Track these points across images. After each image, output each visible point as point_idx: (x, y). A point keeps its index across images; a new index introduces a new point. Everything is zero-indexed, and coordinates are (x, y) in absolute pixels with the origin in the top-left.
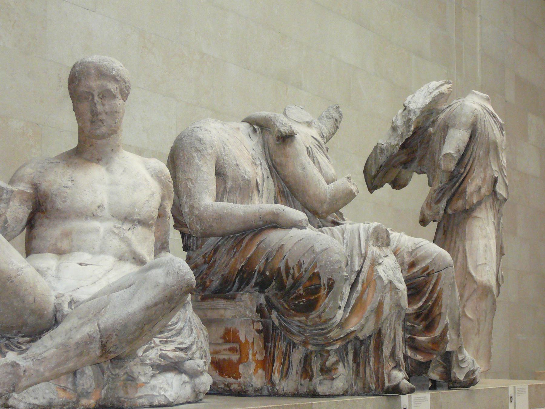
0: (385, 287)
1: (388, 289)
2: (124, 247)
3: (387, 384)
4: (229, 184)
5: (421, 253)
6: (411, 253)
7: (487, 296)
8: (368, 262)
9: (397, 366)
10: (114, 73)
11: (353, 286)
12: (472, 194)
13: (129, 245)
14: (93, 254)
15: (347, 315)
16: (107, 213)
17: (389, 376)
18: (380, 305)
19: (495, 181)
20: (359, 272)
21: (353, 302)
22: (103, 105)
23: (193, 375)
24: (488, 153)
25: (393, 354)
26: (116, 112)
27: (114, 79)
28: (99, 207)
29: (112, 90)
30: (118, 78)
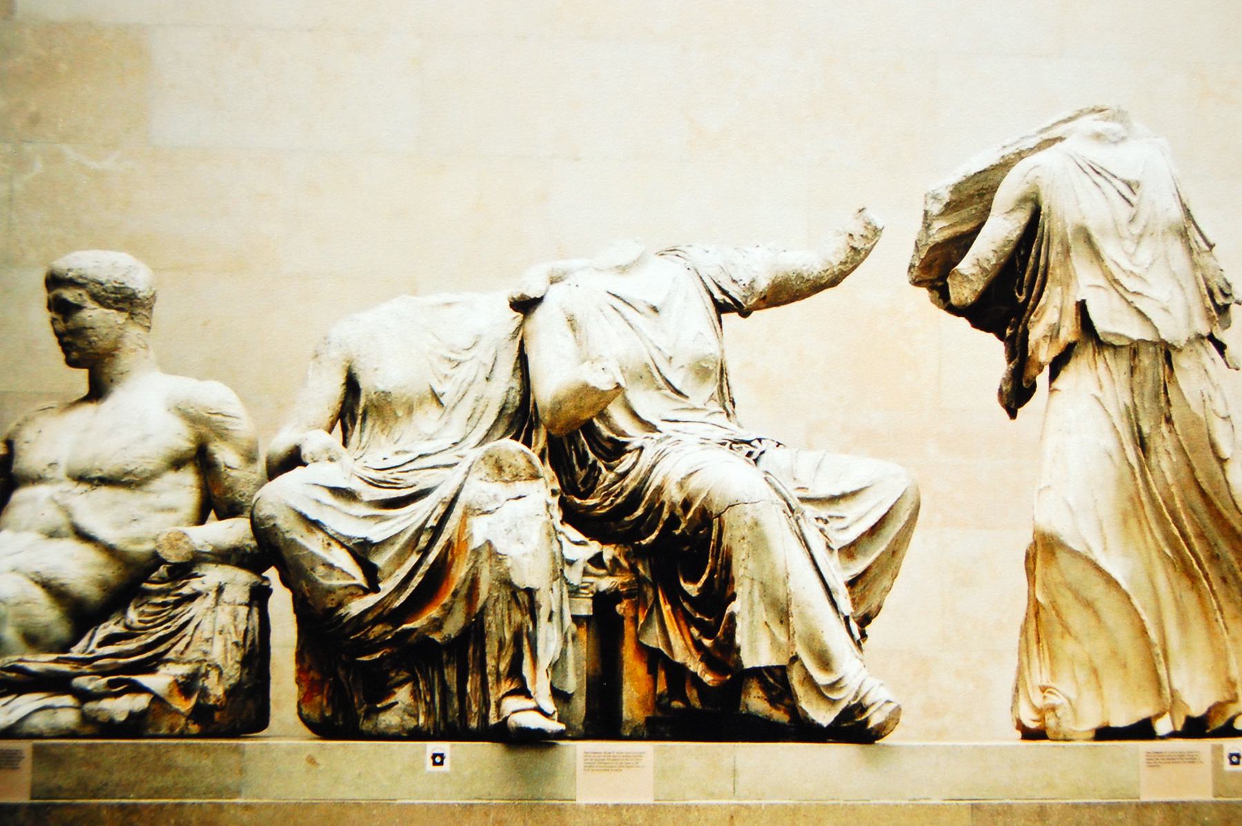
0: (477, 552)
1: (485, 555)
2: (60, 520)
3: (493, 720)
4: (362, 402)
5: (693, 484)
6: (681, 485)
7: (1053, 554)
8: (458, 511)
9: (523, 691)
10: (70, 275)
11: (426, 552)
12: (1037, 344)
13: (69, 515)
14: (17, 530)
15: (397, 604)
16: (61, 472)
17: (498, 705)
18: (473, 583)
19: (1082, 307)
20: (437, 531)
21: (417, 580)
22: (65, 321)
23: (84, 696)
24: (1067, 251)
25: (515, 670)
26: (85, 328)
27: (71, 283)
28: (50, 465)
29: (71, 299)
30: (80, 281)
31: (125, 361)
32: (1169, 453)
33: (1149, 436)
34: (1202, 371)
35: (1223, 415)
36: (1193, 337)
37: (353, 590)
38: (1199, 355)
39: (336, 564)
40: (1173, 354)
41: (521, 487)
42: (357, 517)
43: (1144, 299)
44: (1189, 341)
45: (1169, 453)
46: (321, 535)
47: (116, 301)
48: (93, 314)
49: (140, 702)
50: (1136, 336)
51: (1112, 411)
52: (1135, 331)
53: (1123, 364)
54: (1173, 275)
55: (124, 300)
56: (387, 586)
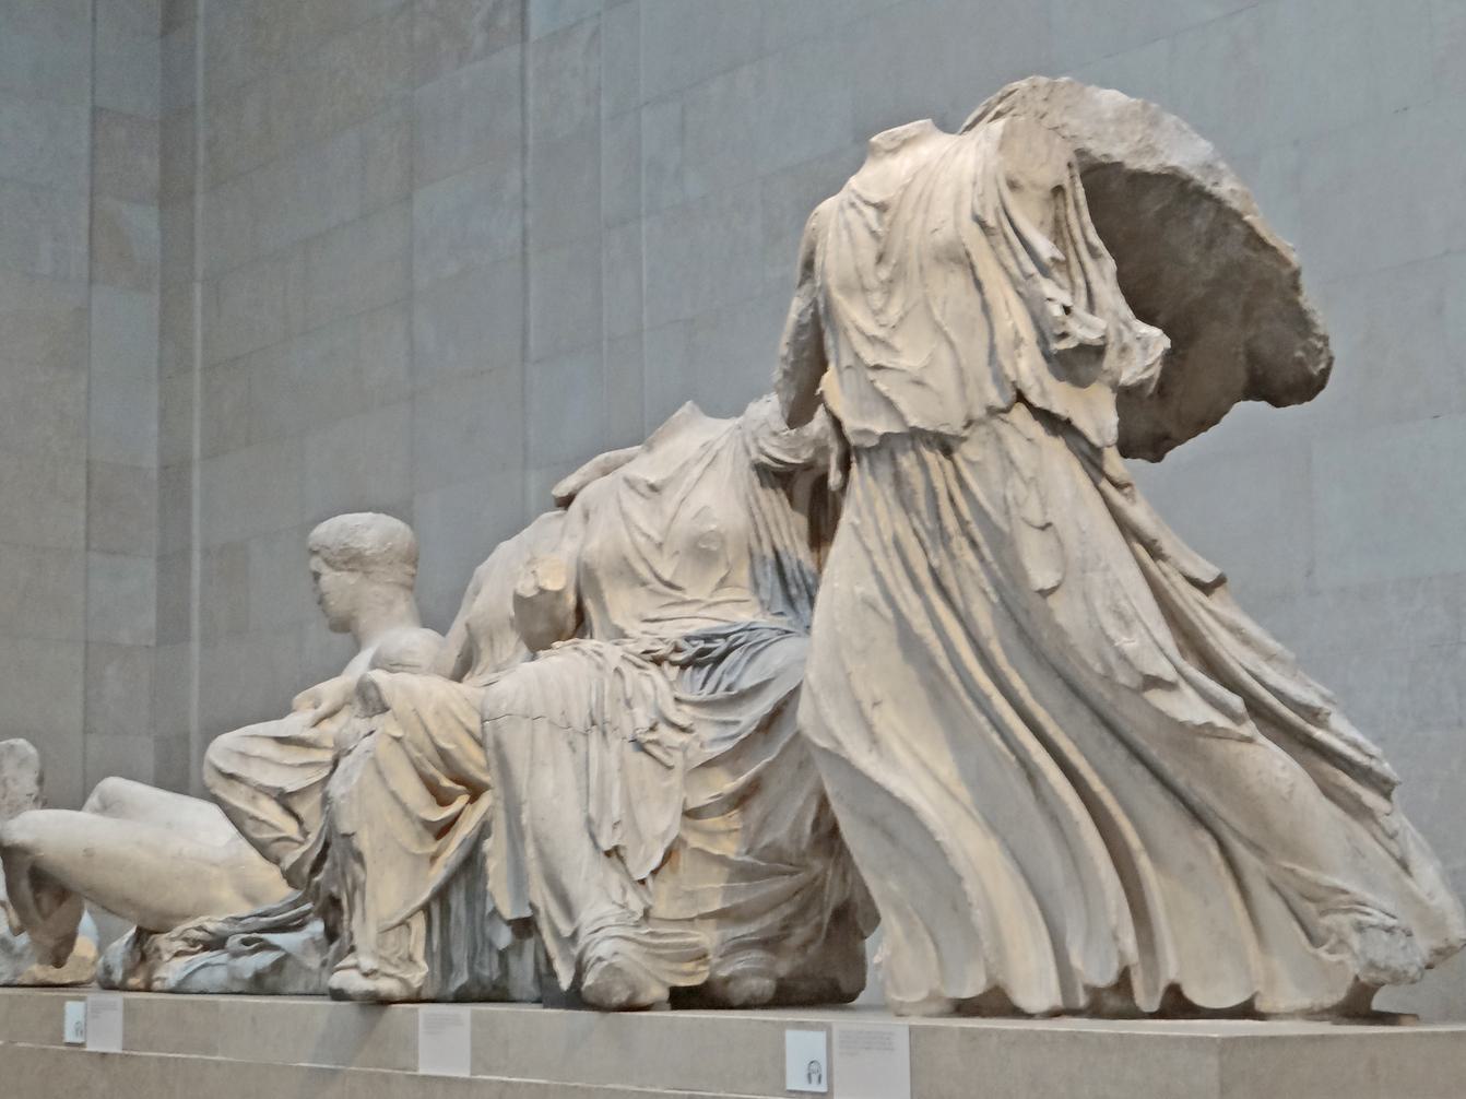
30: (316, 549)
31: (364, 620)
32: (984, 592)
33: (941, 566)
34: (1007, 463)
35: (1039, 521)
36: (979, 412)
37: (287, 843)
38: (999, 439)
39: (263, 816)
40: (953, 443)
41: (378, 721)
42: (291, 766)
43: (888, 375)
44: (969, 423)
45: (984, 592)
46: (243, 788)
47: (345, 563)
48: (329, 577)
49: (264, 959)
50: (880, 429)
51: (873, 543)
52: (881, 425)
53: (885, 470)
54: (938, 328)
55: (352, 560)
56: (312, 837)
